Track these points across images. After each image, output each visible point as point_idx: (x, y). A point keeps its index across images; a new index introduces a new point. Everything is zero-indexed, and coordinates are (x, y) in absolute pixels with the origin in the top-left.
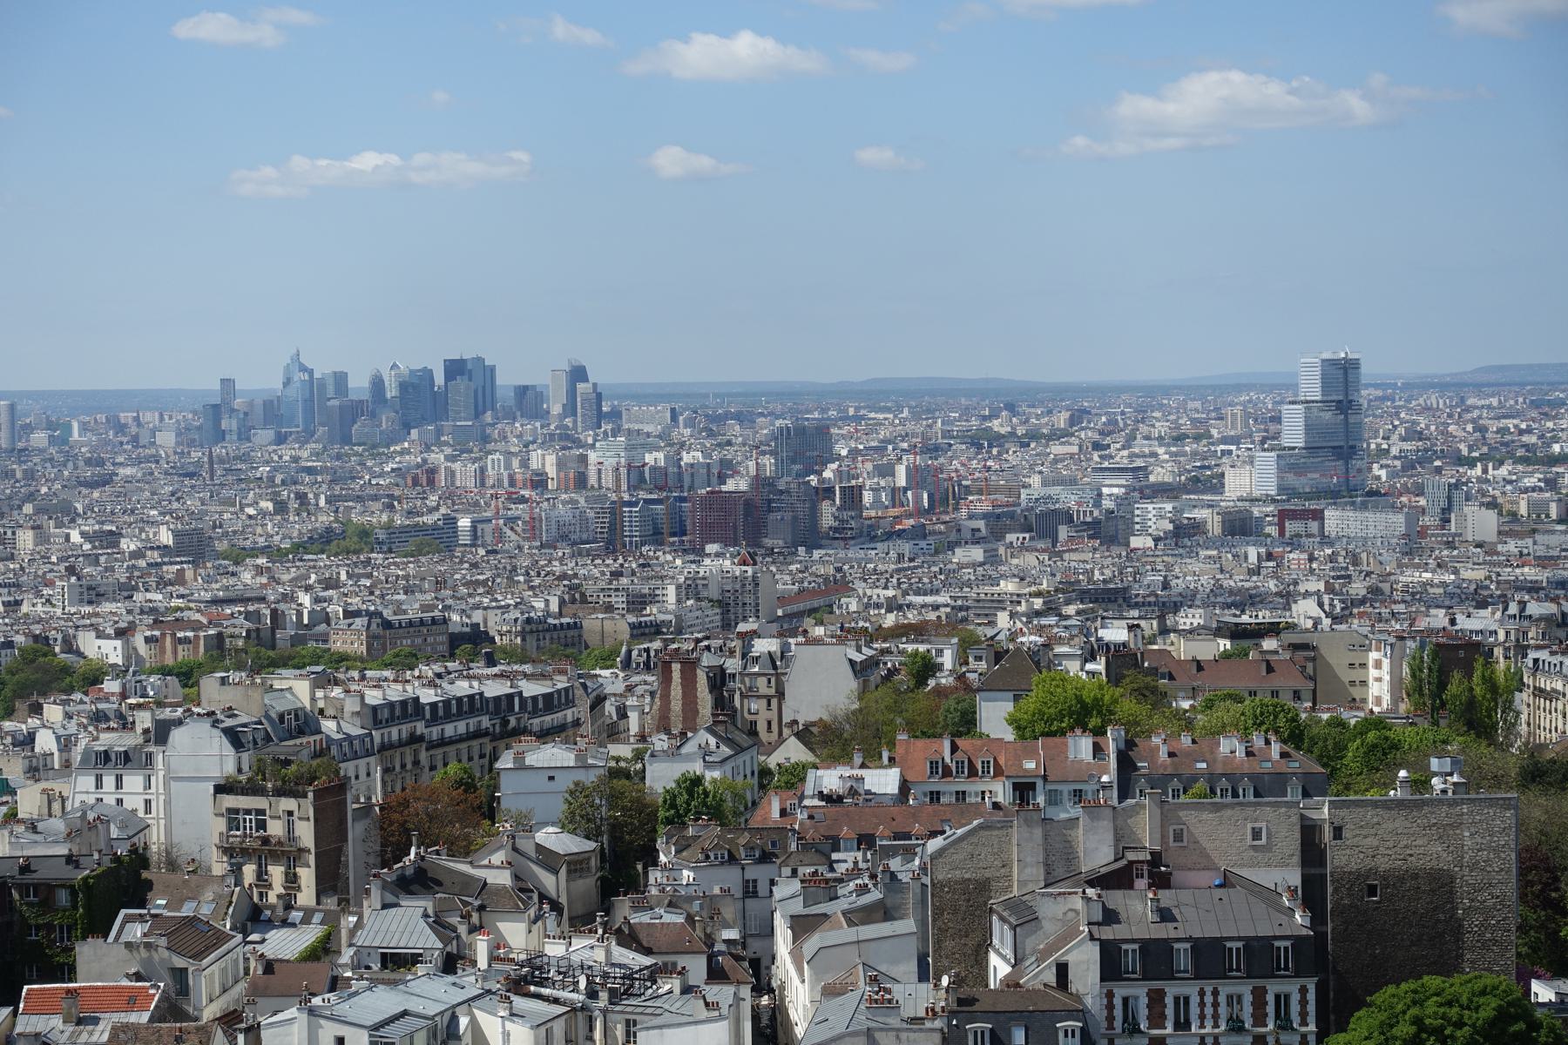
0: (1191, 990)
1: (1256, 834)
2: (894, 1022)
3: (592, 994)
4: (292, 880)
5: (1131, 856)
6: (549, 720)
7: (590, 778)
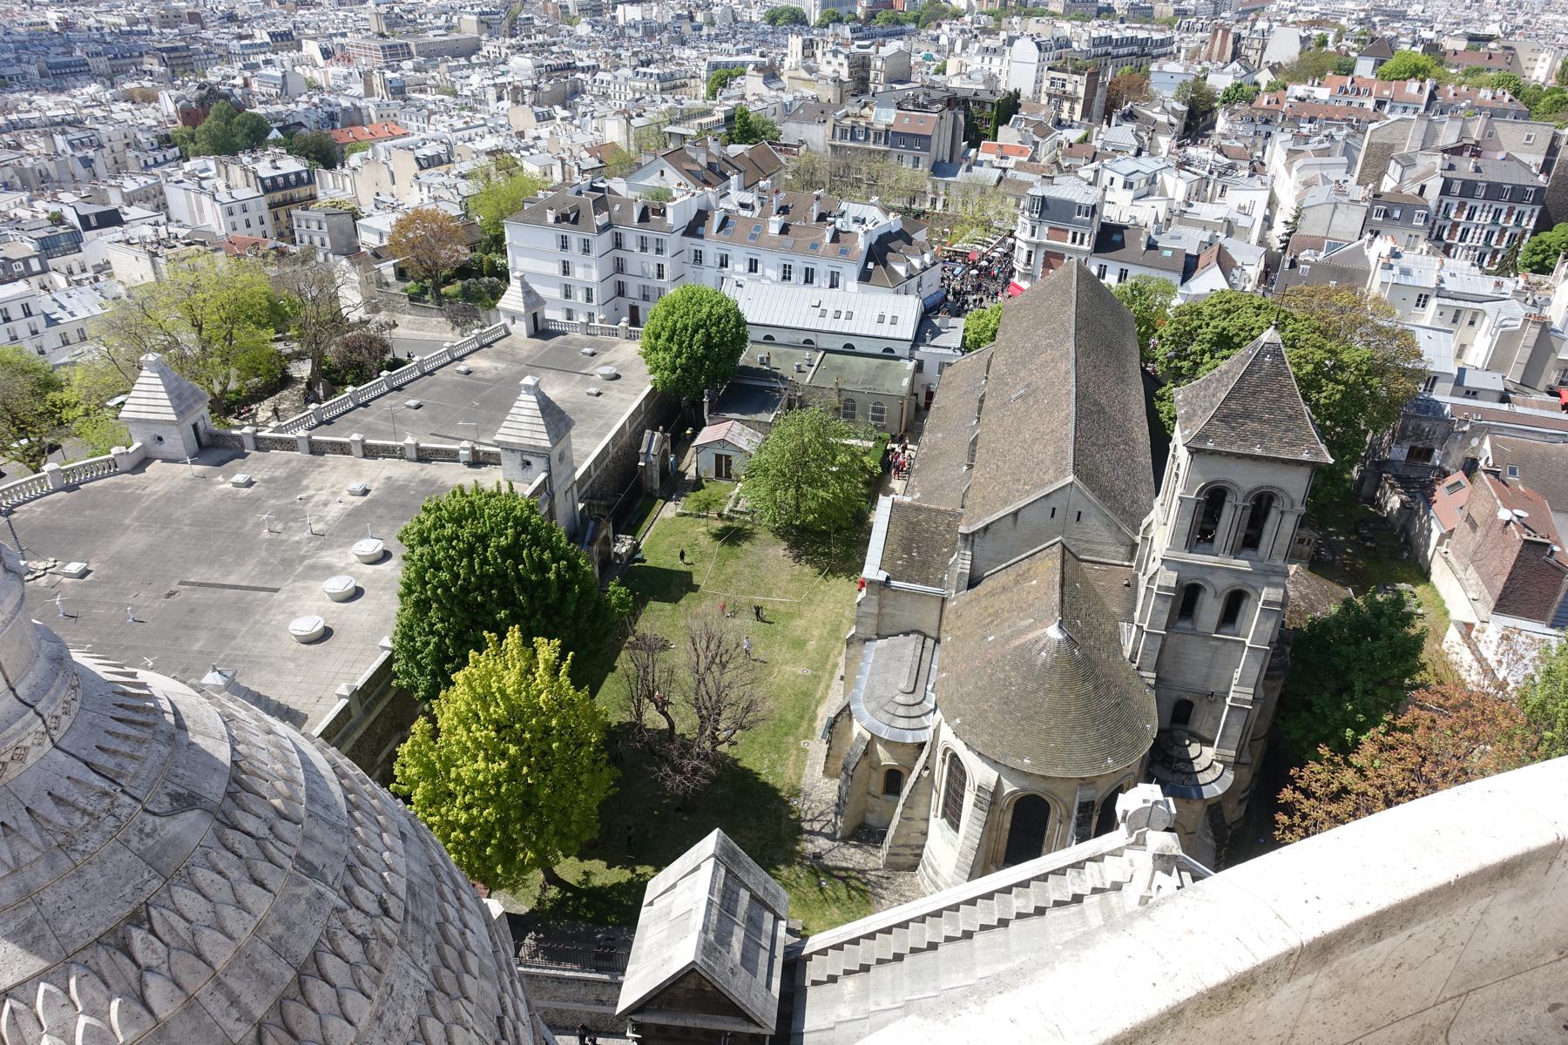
0: (1480, 204)
1: (1529, 138)
2: (1345, 199)
3: (1211, 172)
4: (1072, 110)
5: (1465, 141)
6: (1161, 50)
7: (1190, 79)
